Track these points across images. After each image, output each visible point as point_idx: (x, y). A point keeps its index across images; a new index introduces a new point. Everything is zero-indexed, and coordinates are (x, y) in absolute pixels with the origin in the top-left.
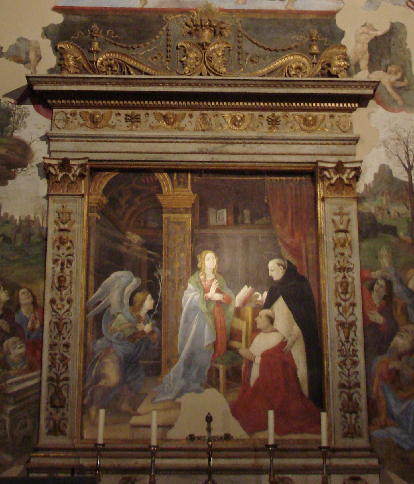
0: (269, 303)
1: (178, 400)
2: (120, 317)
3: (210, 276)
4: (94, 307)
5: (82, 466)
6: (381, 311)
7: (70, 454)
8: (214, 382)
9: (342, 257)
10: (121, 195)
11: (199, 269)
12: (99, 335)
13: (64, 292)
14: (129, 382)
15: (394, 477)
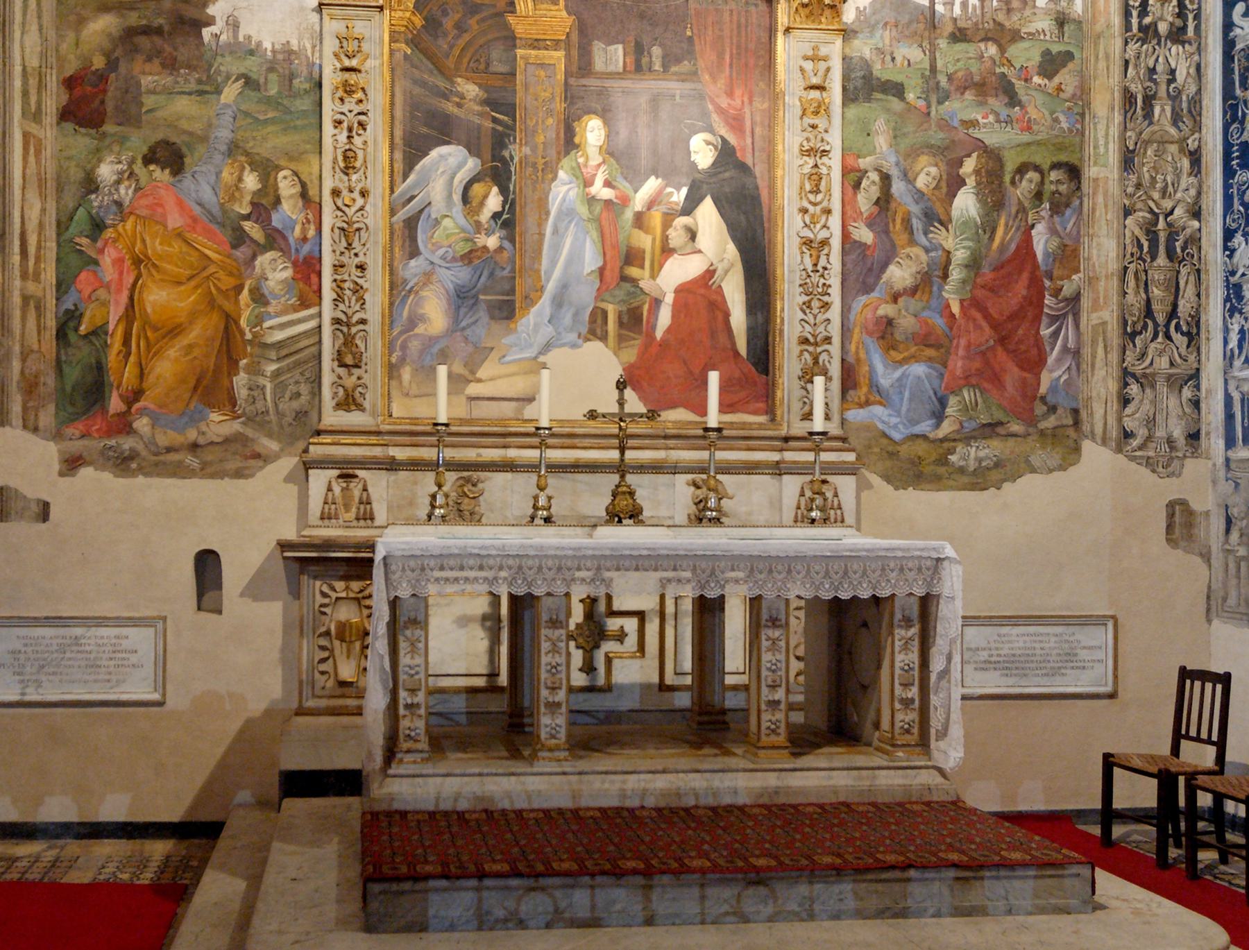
0: (689, 208)
1: (542, 359)
2: (447, 222)
3: (595, 159)
4: (404, 205)
5: (393, 458)
6: (870, 225)
7: (373, 439)
8: (599, 332)
9: (815, 132)
10: (445, 13)
11: (577, 147)
12: (414, 253)
13: (354, 177)
14: (464, 329)
15: (875, 480)
